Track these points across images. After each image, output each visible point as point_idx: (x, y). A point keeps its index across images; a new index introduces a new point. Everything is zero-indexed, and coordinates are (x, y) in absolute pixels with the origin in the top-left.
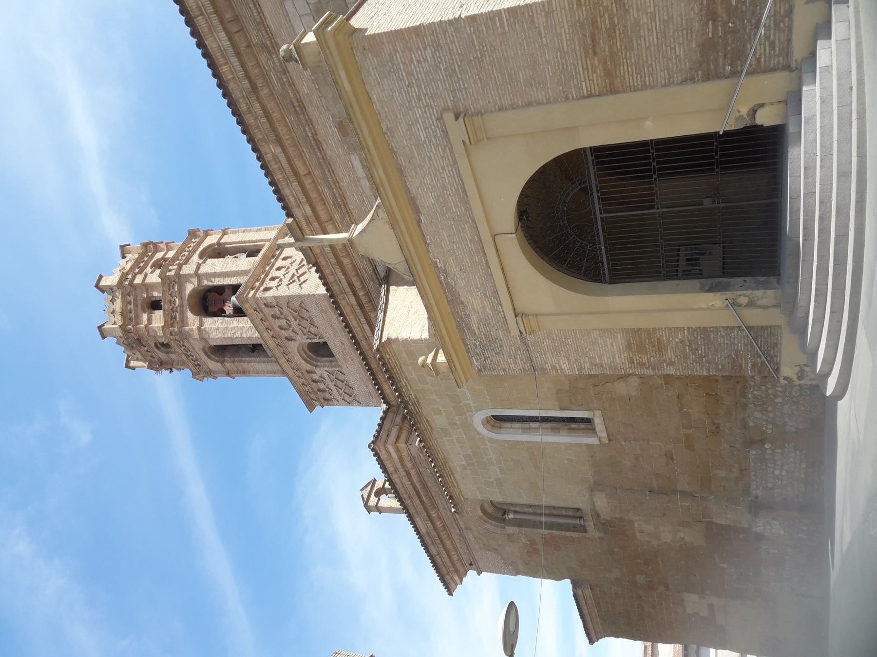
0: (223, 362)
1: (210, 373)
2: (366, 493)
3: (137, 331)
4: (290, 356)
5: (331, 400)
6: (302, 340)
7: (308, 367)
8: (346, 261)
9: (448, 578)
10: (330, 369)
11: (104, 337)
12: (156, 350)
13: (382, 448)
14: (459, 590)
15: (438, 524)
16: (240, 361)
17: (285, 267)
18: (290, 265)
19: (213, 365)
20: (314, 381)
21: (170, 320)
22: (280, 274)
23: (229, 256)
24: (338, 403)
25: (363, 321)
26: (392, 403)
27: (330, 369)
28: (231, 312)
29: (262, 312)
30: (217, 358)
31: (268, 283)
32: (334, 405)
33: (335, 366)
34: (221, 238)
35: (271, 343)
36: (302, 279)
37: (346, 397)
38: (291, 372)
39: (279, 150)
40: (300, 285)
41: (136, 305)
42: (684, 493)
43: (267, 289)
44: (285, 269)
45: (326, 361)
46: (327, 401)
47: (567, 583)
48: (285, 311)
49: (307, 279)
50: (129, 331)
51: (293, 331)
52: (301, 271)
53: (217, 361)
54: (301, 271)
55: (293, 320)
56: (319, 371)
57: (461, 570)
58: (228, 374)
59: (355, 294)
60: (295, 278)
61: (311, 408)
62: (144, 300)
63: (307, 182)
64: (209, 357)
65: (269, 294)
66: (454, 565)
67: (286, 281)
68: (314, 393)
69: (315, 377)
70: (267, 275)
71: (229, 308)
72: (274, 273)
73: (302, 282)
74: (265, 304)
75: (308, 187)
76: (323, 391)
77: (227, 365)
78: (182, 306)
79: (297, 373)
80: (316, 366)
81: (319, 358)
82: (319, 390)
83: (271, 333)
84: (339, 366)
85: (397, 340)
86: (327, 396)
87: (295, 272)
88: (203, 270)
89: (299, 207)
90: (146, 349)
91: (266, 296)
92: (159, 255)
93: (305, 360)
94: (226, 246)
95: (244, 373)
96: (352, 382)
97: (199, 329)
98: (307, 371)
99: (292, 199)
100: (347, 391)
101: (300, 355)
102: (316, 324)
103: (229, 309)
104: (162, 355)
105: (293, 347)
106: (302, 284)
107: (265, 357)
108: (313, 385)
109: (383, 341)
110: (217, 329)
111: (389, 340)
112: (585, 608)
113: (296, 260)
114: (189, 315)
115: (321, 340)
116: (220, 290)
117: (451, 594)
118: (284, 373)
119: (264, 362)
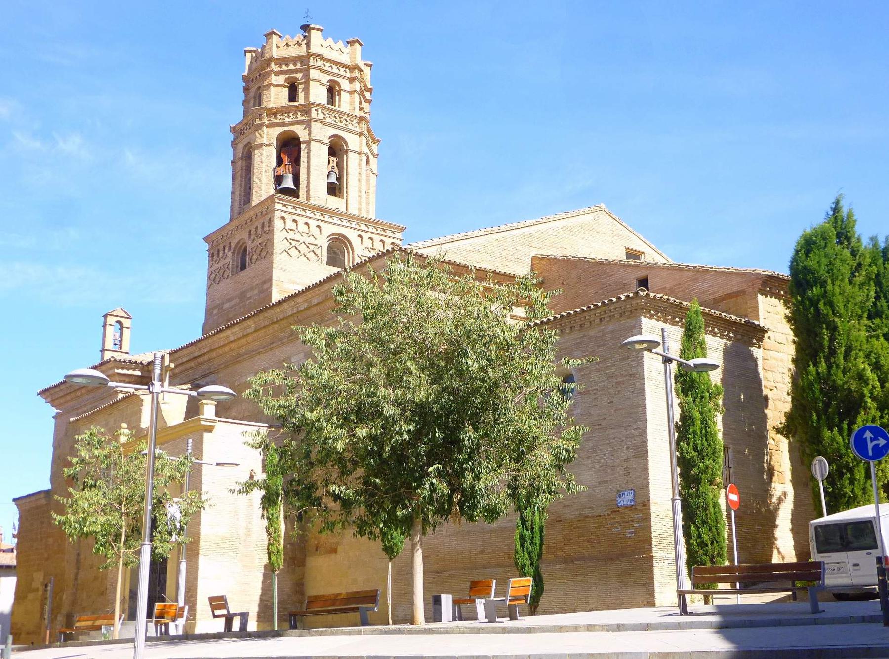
0: (242, 158)
1: (234, 144)
2: (119, 312)
3: (269, 74)
4: (240, 230)
5: (212, 260)
6: (250, 245)
7: (233, 245)
9: (48, 394)
10: (230, 266)
11: (265, 35)
12: (256, 87)
13: (113, 365)
14: (41, 400)
15: (79, 393)
16: (242, 177)
18: (310, 234)
19: (240, 146)
20: (224, 247)
21: (272, 113)
22: (302, 228)
23: (335, 163)
24: (211, 267)
27: (230, 266)
28: (278, 174)
29: (266, 214)
30: (245, 153)
32: (209, 262)
33: (232, 271)
34: (353, 151)
35: (247, 216)
36: (293, 252)
37: (213, 276)
38: (230, 228)
39: (253, 330)
41: (292, 71)
42: (77, 574)
43: (283, 218)
45: (237, 262)
46: (212, 256)
47: (48, 486)
48: (266, 236)
50: (269, 65)
51: (254, 239)
52: (303, 248)
53: (243, 153)
54: (303, 248)
55: (260, 241)
56: (229, 254)
57: (57, 402)
58: (232, 163)
59: (200, 356)
60: (294, 243)
61: (206, 239)
62: (296, 78)
63: (244, 341)
64: (246, 146)
65: (278, 224)
66: (57, 399)
67: (291, 235)
68: (217, 246)
69: (227, 249)
72: (301, 221)
73: (289, 251)
74: (270, 218)
75: (243, 340)
76: (218, 256)
77: (239, 163)
78: (284, 125)
79: (229, 233)
80: (233, 253)
81: (240, 256)
82: (219, 251)
83: (254, 218)
84: (236, 273)
85: (142, 405)
86: (215, 257)
87: (301, 242)
88: (314, 145)
89: (232, 333)
90: (258, 76)
91: (275, 221)
92: (345, 85)
93: (238, 243)
94: (345, 156)
95: (233, 179)
96: (222, 284)
97: (262, 145)
98: (230, 243)
99: (234, 331)
100: (217, 277)
101: (240, 241)
102: (257, 263)
103: (280, 171)
104: (252, 92)
105: (245, 235)
107: (245, 201)
108: (221, 247)
109: (141, 397)
110: (262, 162)
111: (142, 400)
112: (33, 498)
113: (316, 239)
114: (278, 131)
115: (247, 264)
116: (296, 161)
117: (38, 394)
118: (231, 218)
119: (240, 201)
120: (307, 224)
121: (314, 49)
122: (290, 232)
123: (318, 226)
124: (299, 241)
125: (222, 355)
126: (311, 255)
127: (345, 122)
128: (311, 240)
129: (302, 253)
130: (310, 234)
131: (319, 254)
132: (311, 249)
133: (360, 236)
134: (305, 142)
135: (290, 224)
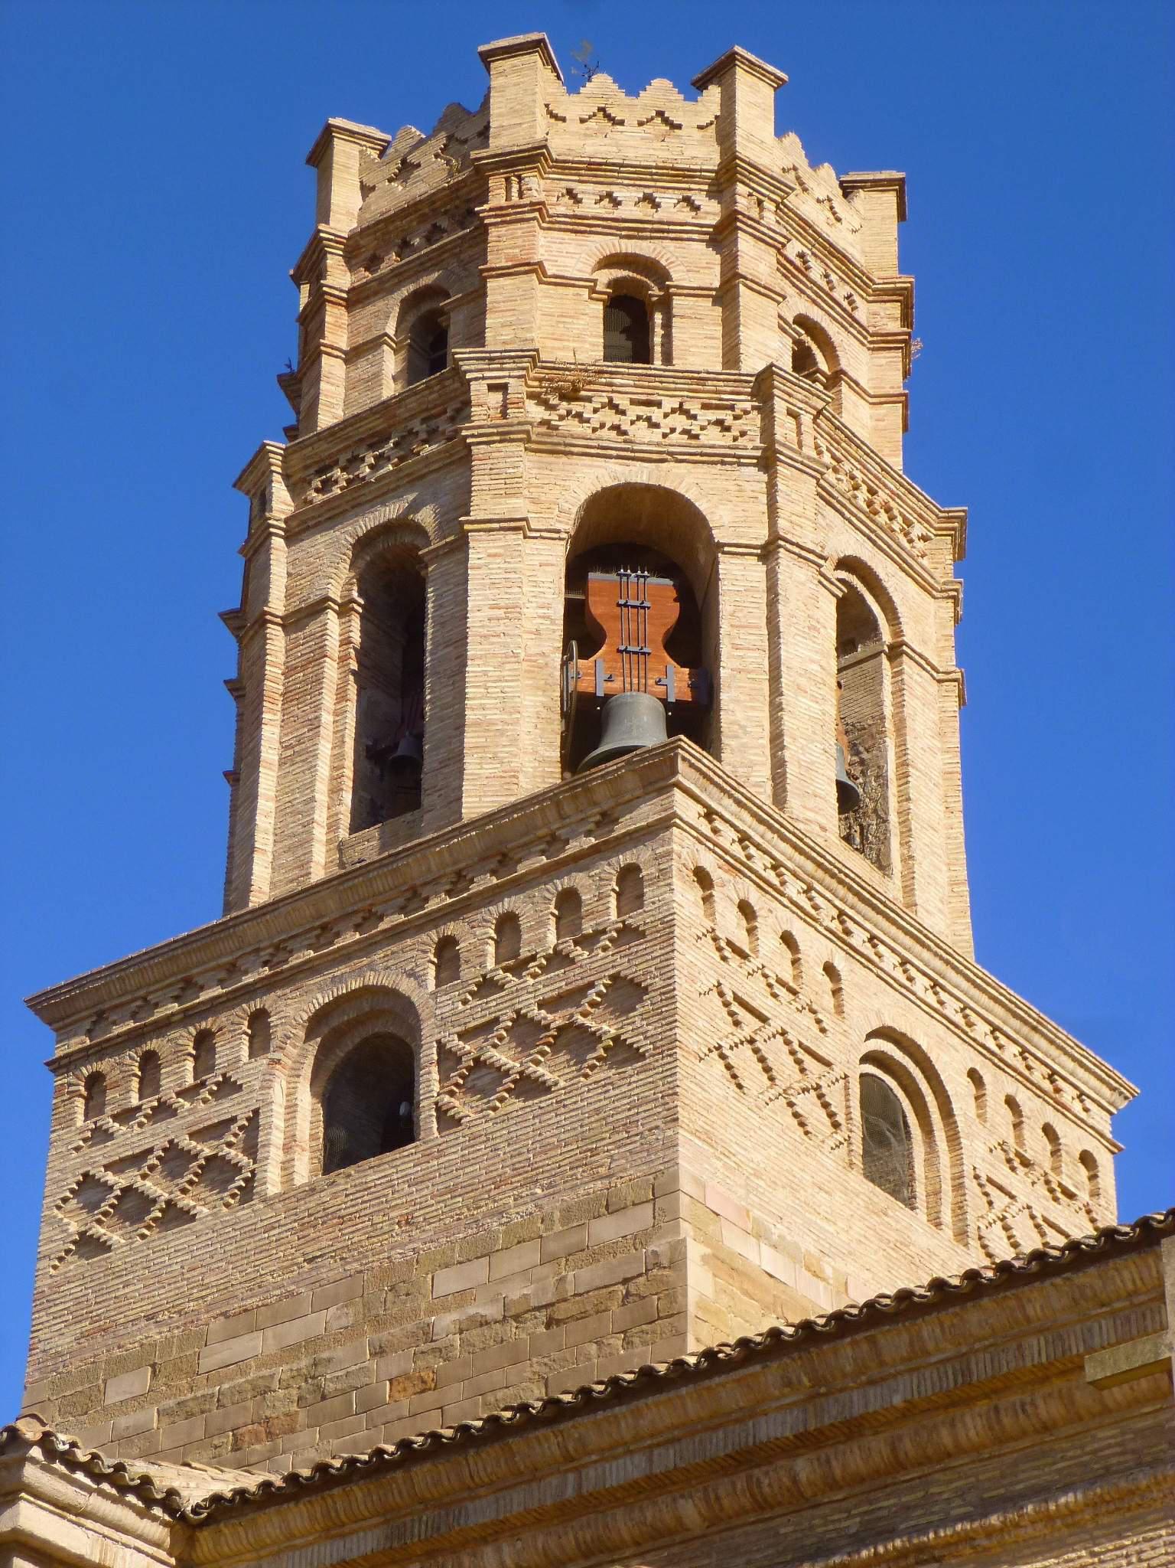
8: (972, 1426)
17: (797, 977)
22: (770, 950)
25: (666, 1460)
26: (204, 1536)
28: (585, 686)
31: (729, 889)
36: (744, 1060)
40: (719, 1048)
41: (636, 230)
43: (702, 877)
44: (788, 975)
49: (740, 1086)
59: (807, 1441)
60: (750, 1023)
65: (685, 897)
67: (738, 979)
70: (763, 885)
71: (602, 675)
72: (773, 918)
78: (631, 454)
87: (775, 1025)
88: (792, 572)
106: (723, 1057)
120: (788, 939)
121: (745, 148)
122: (735, 960)
123: (830, 970)
124: (763, 1019)
125: (1046, 1428)
126: (807, 1104)
127: (883, 518)
128: (803, 1029)
129: (782, 1083)
130: (803, 999)
131: (841, 1118)
132: (812, 1080)
133: (974, 1075)
134: (740, 550)
135: (732, 925)
